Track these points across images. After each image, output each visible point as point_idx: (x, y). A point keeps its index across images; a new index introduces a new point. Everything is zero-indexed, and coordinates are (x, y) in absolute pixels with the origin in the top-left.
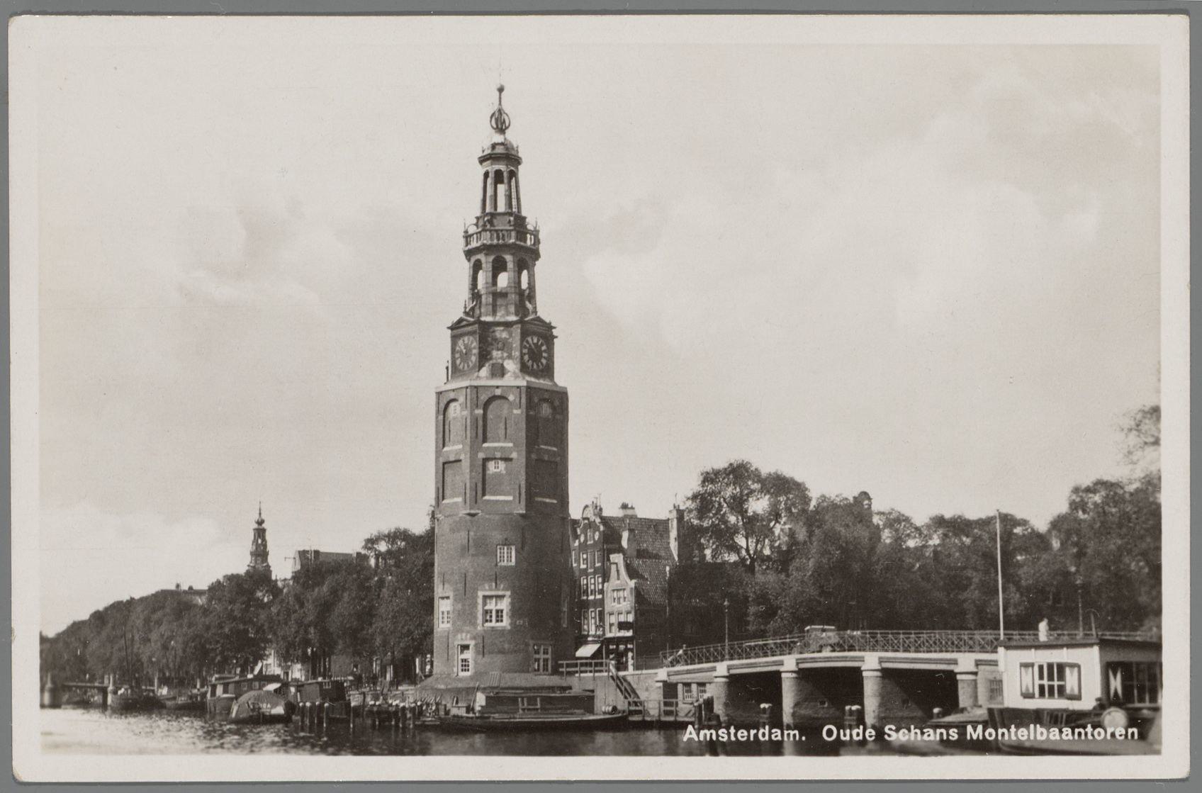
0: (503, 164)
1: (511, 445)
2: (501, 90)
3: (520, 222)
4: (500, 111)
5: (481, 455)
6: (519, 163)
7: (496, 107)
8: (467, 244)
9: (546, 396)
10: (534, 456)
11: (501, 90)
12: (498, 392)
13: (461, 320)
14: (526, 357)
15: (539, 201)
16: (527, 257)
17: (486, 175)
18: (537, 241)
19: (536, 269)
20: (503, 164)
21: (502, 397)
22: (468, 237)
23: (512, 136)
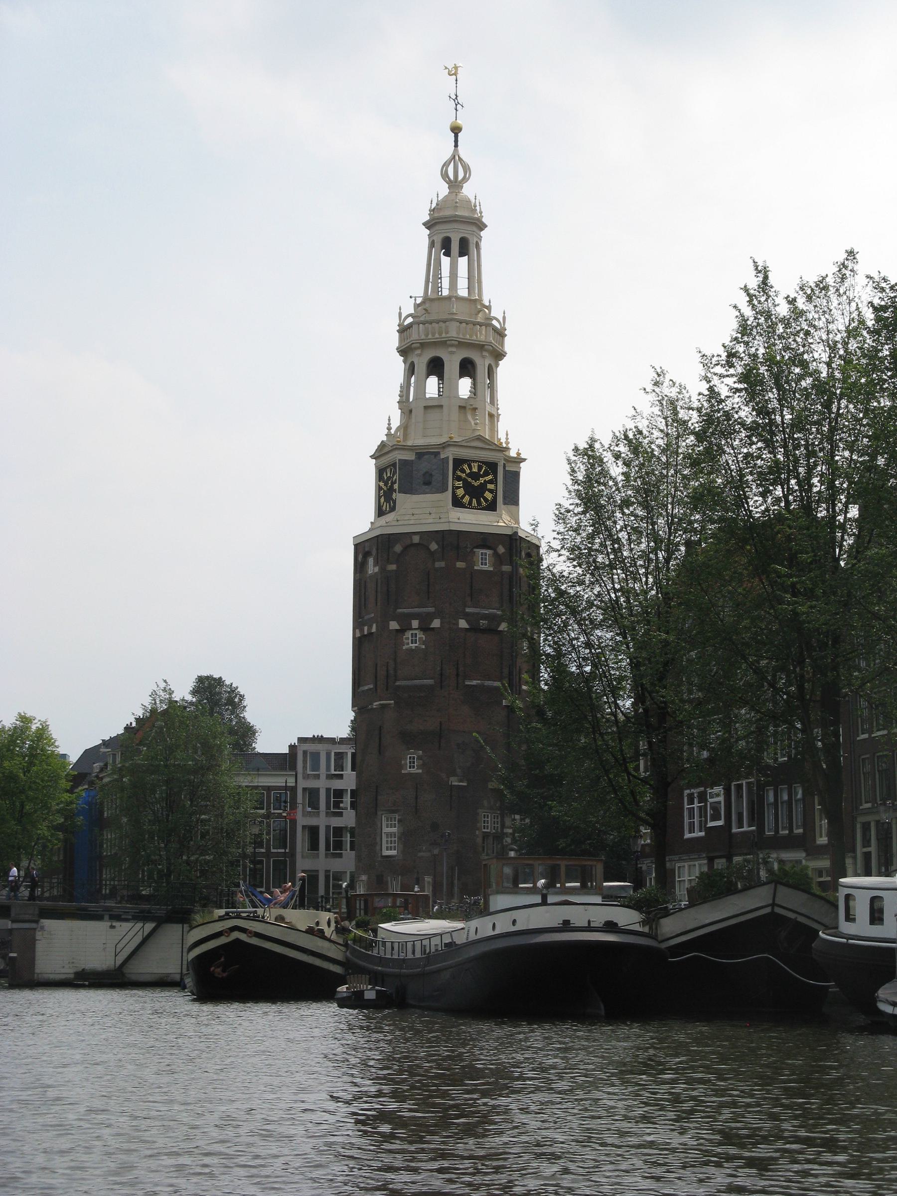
0: (454, 231)
2: (456, 130)
4: (455, 158)
6: (481, 226)
8: (401, 340)
11: (456, 130)
12: (416, 539)
13: (383, 445)
14: (460, 492)
15: (505, 281)
17: (432, 245)
18: (500, 334)
20: (454, 231)
22: (403, 330)
23: (468, 191)
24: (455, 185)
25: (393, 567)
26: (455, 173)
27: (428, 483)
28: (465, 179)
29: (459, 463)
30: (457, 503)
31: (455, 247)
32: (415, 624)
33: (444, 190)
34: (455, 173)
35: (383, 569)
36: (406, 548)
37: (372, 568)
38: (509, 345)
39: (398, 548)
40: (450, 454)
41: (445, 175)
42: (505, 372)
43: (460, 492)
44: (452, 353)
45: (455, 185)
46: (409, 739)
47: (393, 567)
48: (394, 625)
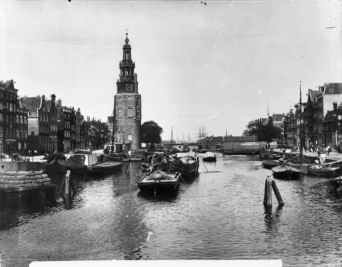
2: (127, 34)
3: (130, 61)
4: (127, 39)
5: (118, 108)
7: (126, 38)
9: (130, 96)
10: (127, 108)
11: (127, 34)
12: (120, 96)
16: (133, 67)
18: (134, 65)
19: (134, 70)
20: (127, 49)
21: (121, 97)
22: (120, 65)
23: (129, 43)
26: (127, 40)
33: (125, 43)
34: (127, 40)
38: (135, 66)
41: (125, 42)
42: (135, 71)
44: (126, 69)
45: (127, 43)
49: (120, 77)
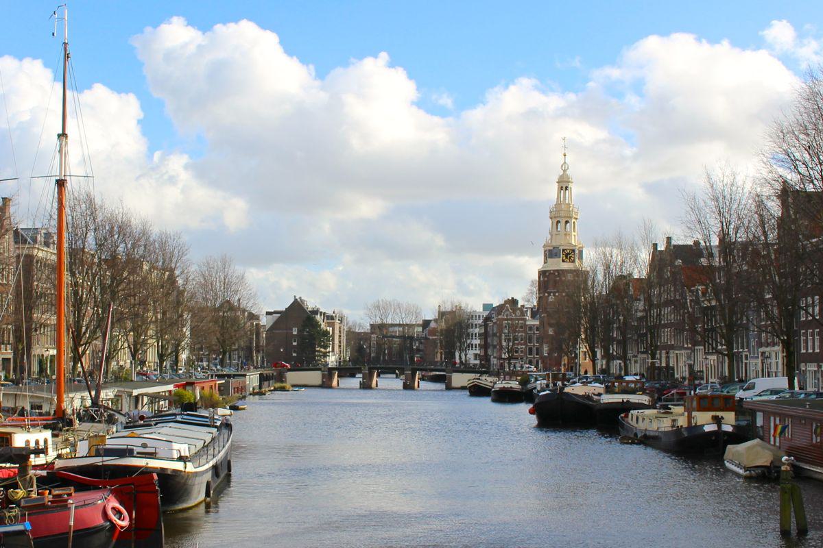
1: (555, 290)
2: (565, 155)
14: (564, 258)
22: (551, 212)
23: (568, 172)
24: (565, 171)
25: (546, 279)
27: (556, 255)
28: (568, 168)
29: (563, 250)
30: (563, 261)
31: (564, 188)
32: (552, 294)
35: (544, 279)
36: (549, 274)
37: (542, 279)
39: (547, 274)
40: (561, 248)
43: (564, 258)
45: (565, 171)
46: (551, 325)
47: (546, 279)
48: (546, 294)
49: (552, 235)
